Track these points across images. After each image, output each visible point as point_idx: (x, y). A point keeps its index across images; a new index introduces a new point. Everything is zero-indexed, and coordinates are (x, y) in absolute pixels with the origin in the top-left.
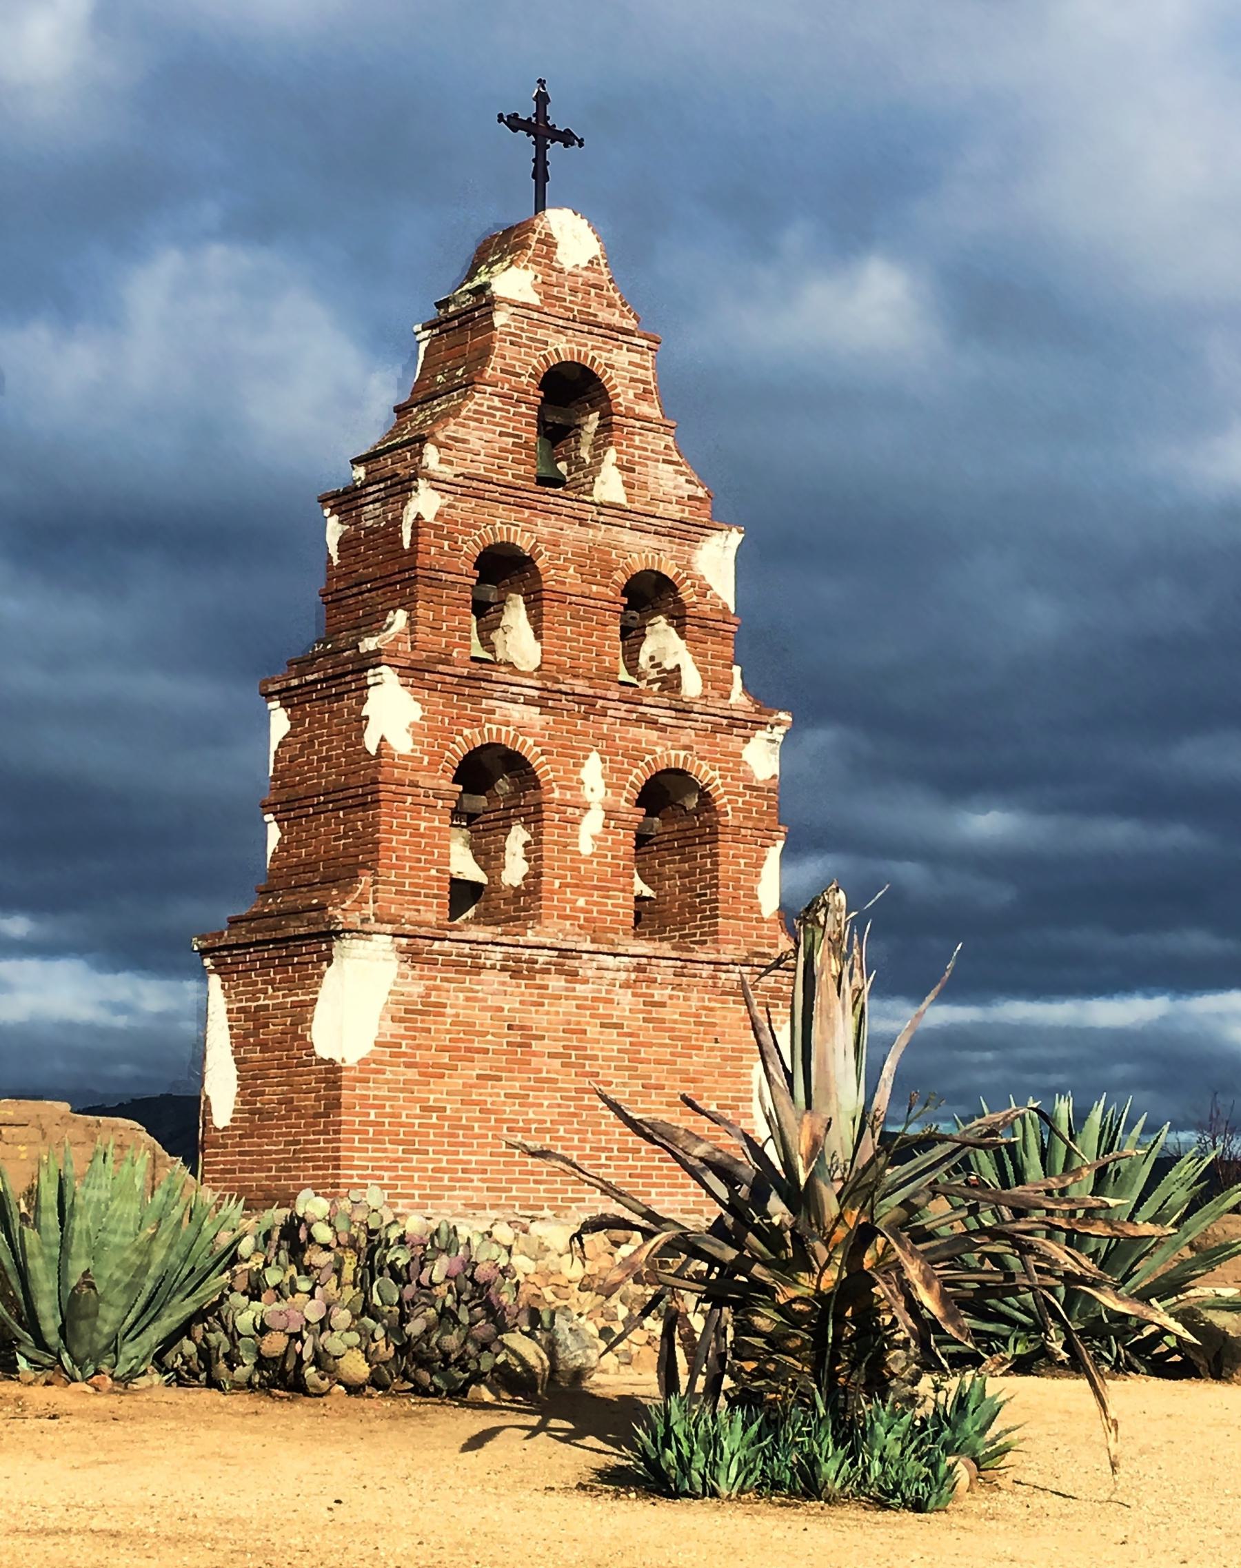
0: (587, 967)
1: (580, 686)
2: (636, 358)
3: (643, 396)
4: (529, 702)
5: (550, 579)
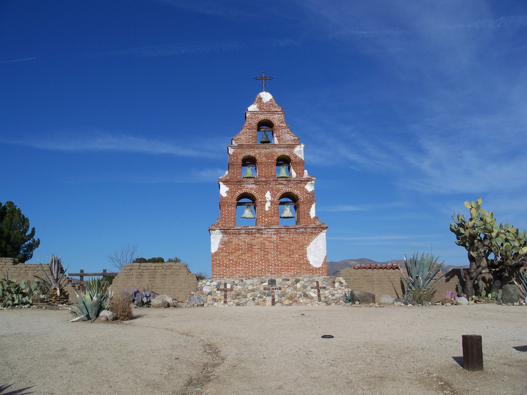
0: (265, 232)
1: (263, 179)
2: (280, 116)
3: (282, 122)
4: (252, 184)
5: (259, 160)
